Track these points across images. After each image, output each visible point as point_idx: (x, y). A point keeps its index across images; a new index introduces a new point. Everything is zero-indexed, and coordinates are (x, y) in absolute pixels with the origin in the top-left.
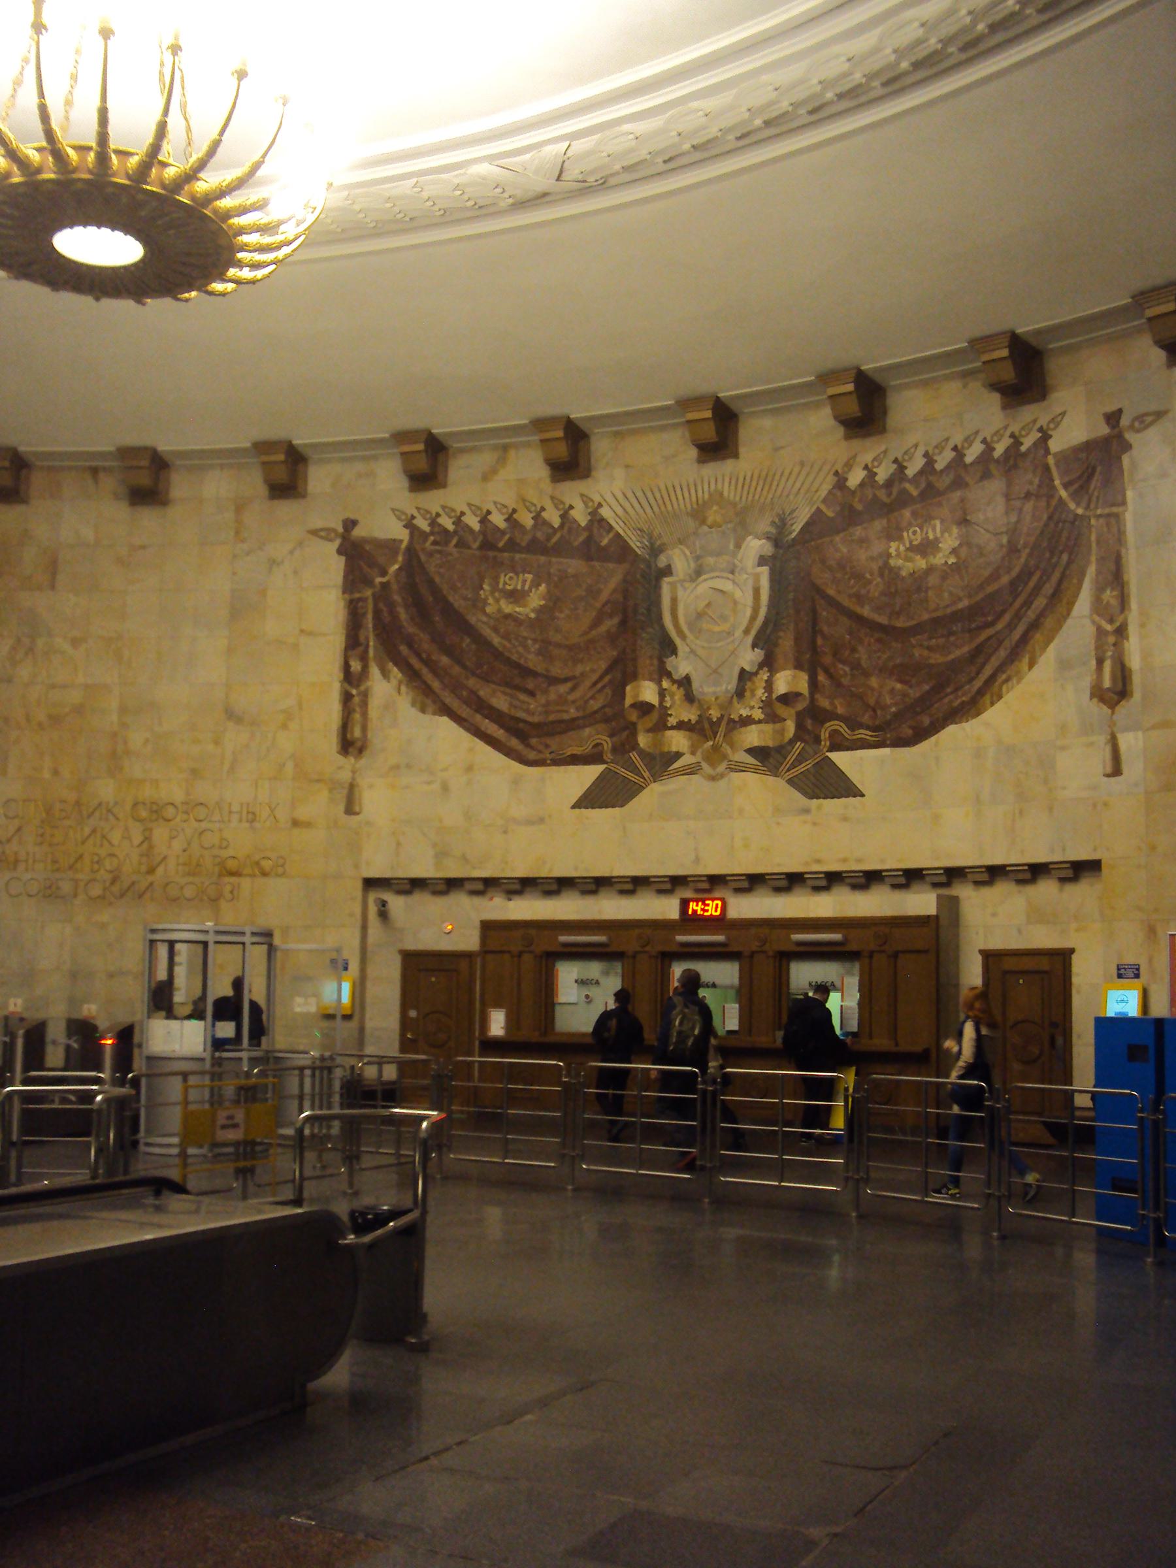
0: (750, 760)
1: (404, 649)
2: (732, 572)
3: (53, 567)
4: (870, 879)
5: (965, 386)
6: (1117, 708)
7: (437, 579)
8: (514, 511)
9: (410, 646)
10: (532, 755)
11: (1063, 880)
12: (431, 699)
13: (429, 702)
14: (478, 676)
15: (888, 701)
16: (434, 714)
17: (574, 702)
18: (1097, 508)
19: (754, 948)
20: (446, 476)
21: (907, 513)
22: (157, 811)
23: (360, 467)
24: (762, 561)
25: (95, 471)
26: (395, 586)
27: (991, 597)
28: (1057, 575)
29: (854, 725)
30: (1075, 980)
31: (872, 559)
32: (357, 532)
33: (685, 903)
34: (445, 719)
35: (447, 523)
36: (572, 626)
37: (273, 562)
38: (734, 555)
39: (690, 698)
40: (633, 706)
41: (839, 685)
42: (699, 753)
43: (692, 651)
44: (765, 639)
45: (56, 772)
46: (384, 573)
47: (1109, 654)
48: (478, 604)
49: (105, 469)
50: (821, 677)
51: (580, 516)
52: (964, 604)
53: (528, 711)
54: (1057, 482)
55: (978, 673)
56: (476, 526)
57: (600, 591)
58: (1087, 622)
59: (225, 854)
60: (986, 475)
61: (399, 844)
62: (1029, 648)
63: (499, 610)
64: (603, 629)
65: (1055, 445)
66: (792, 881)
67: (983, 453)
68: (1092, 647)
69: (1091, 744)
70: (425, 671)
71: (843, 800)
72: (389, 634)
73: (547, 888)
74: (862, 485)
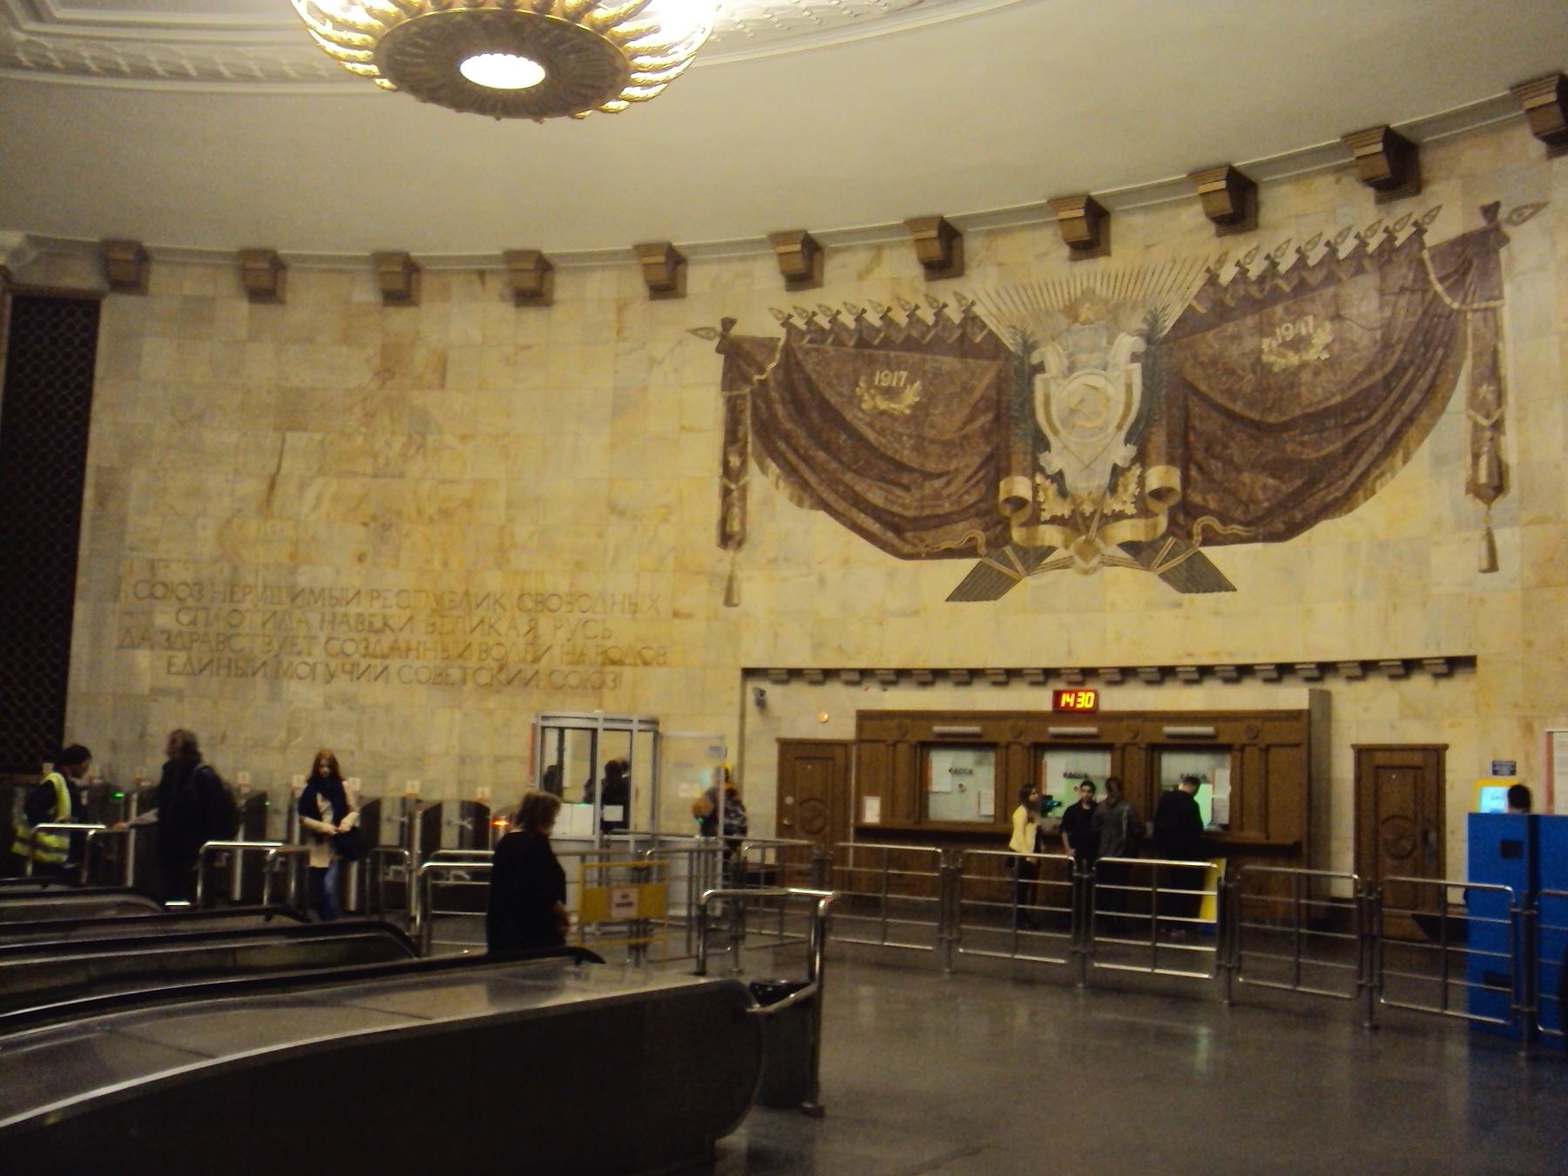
0: (1122, 554)
1: (782, 445)
2: (1105, 369)
3: (442, 367)
4: (1243, 672)
5: (1338, 181)
6: (1495, 505)
7: (814, 377)
8: (889, 309)
9: (788, 443)
10: (907, 549)
11: (1438, 676)
12: (807, 493)
13: (806, 496)
14: (855, 471)
15: (1261, 496)
16: (812, 507)
17: (949, 496)
19: (1125, 740)
20: (822, 275)
21: (1279, 310)
22: (542, 602)
23: (737, 267)
24: (1134, 358)
25: (482, 274)
26: (772, 384)
27: (1366, 394)
28: (1432, 370)
29: (1225, 519)
30: (1449, 776)
31: (1244, 354)
32: (736, 331)
33: (1058, 695)
34: (822, 515)
35: (823, 321)
36: (947, 422)
37: (653, 361)
38: (1106, 351)
39: (1063, 493)
40: (1007, 500)
41: (1211, 480)
42: (1072, 547)
43: (1065, 447)
44: (1138, 435)
45: (445, 564)
46: (761, 370)
48: (855, 401)
49: (493, 272)
50: (1194, 472)
51: (954, 314)
52: (1338, 399)
53: (903, 506)
54: (1432, 277)
55: (1352, 467)
56: (851, 324)
57: (973, 388)
58: (1463, 416)
59: (609, 643)
60: (1360, 270)
61: (776, 635)
62: (1403, 443)
63: (875, 407)
64: (977, 425)
65: (1430, 239)
66: (1165, 674)
67: (1357, 248)
68: (1468, 443)
69: (1466, 540)
70: (803, 468)
71: (1216, 594)
72: (768, 432)
73: (922, 679)
74: (1234, 281)
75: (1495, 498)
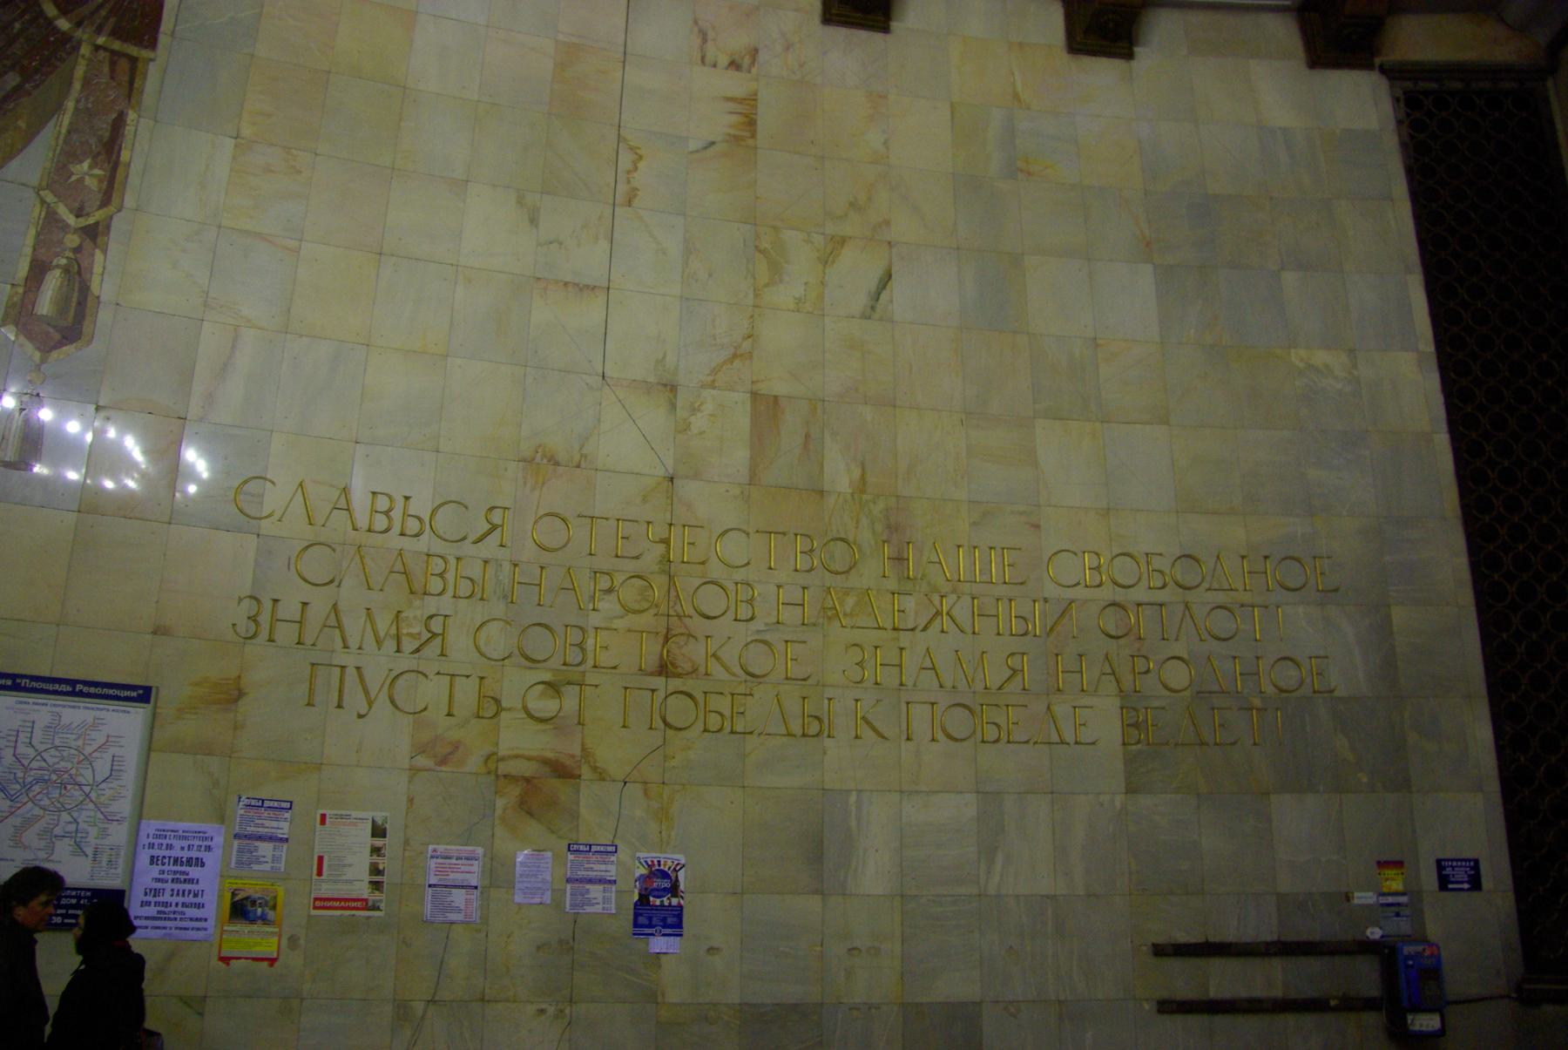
6: (54, 354)
18: (99, 31)
47: (63, 261)
75: (59, 345)
